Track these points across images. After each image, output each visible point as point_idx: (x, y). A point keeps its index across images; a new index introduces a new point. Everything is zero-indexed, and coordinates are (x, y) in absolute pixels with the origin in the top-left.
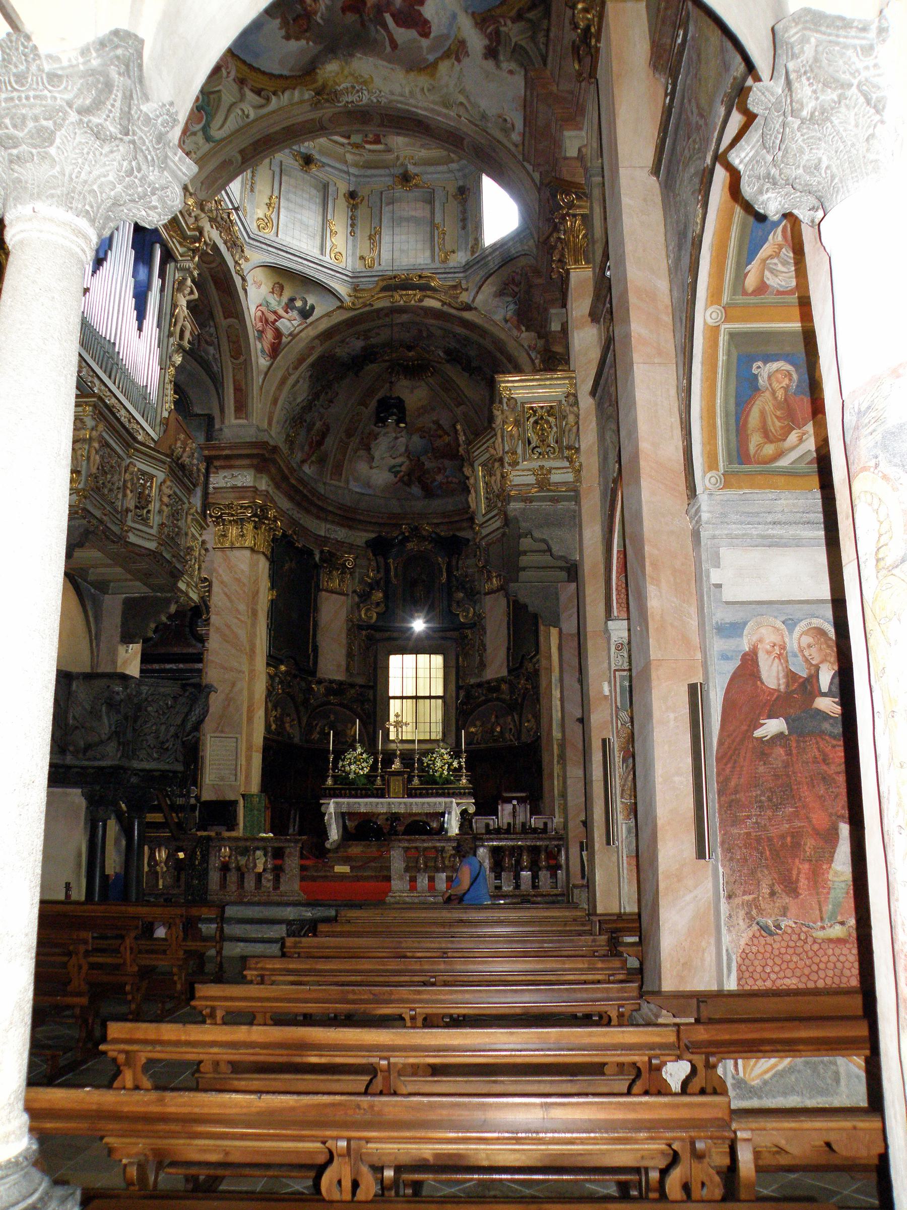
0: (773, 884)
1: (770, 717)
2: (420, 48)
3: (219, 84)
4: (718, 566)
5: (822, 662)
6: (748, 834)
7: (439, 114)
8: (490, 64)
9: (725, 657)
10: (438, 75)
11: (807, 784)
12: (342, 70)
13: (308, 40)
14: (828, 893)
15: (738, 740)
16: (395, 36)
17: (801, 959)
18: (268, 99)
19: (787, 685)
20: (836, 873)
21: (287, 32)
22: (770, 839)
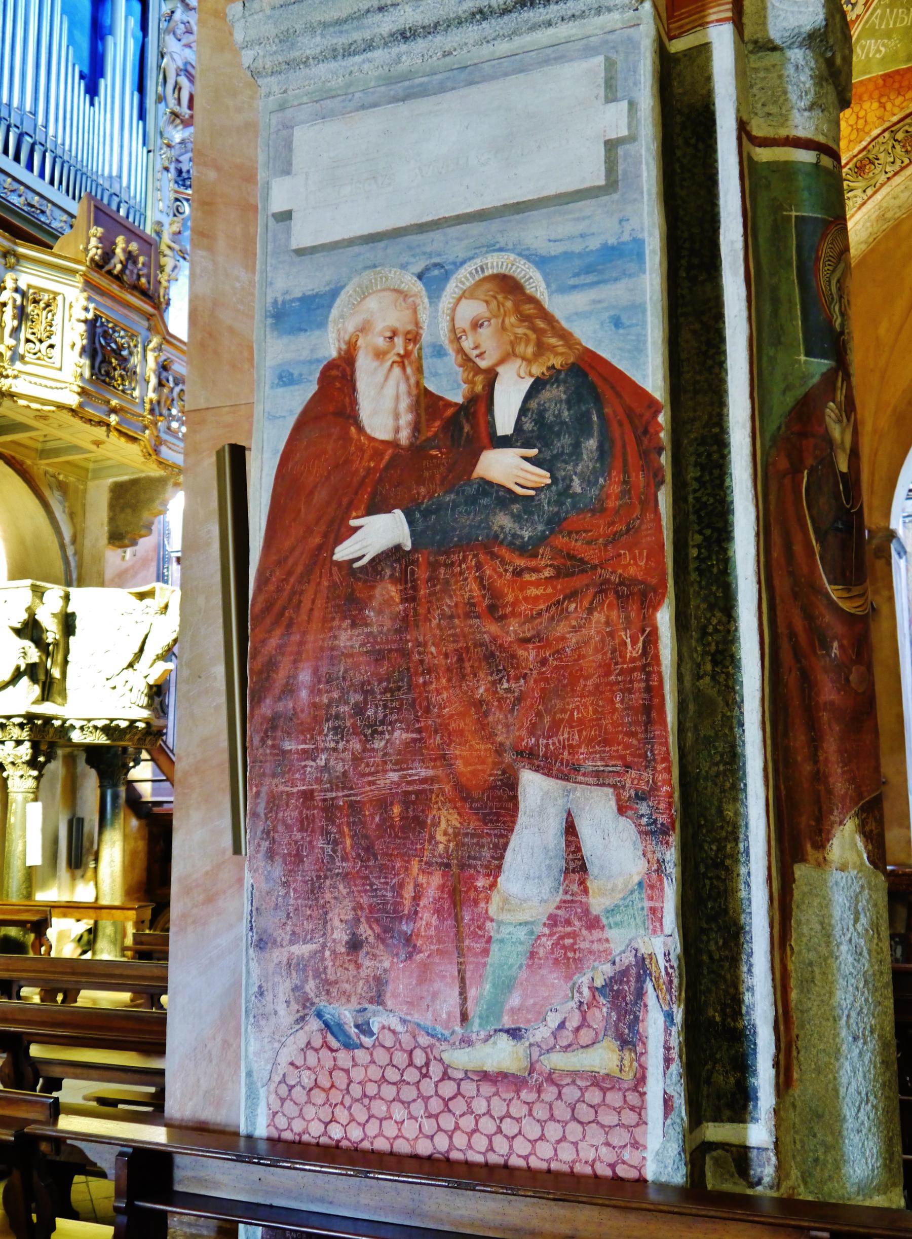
0: (357, 920)
1: (372, 510)
4: (287, 171)
5: (502, 361)
6: (308, 796)
9: (286, 379)
11: (449, 670)
14: (486, 952)
15: (300, 569)
17: (411, 1117)
19: (416, 428)
20: (506, 901)
22: (354, 808)
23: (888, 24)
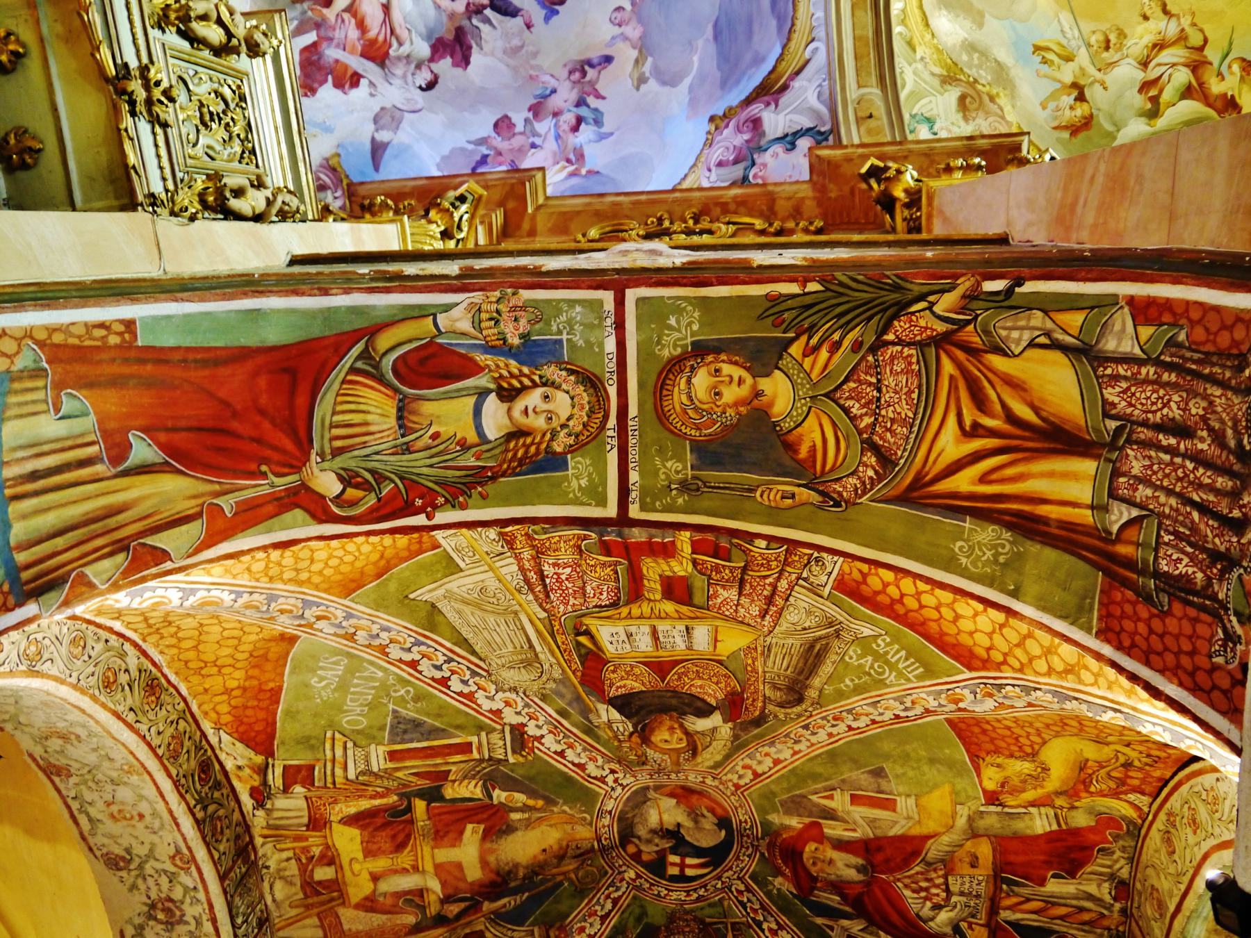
23: (357, 686)
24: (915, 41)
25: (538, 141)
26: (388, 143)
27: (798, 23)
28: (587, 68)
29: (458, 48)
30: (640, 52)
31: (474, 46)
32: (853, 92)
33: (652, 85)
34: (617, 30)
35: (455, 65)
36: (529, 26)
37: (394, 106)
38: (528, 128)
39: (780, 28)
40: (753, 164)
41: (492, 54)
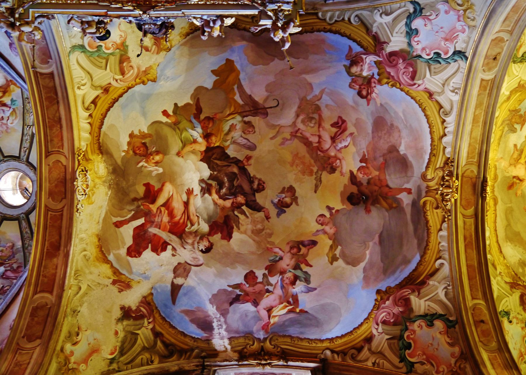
2: (119, 248)
3: (111, 71)
7: (71, 269)
8: (118, 313)
10: (97, 264)
12: (99, 178)
13: (127, 152)
16: (125, 226)
18: (87, 109)
21: (136, 136)
24: (496, 263)
25: (271, 288)
26: (182, 285)
27: (430, 244)
28: (301, 246)
29: (225, 228)
30: (334, 242)
31: (235, 227)
32: (470, 303)
33: (340, 263)
34: (320, 227)
35: (223, 238)
36: (268, 218)
37: (186, 262)
38: (265, 280)
39: (419, 245)
40: (407, 329)
41: (245, 233)
